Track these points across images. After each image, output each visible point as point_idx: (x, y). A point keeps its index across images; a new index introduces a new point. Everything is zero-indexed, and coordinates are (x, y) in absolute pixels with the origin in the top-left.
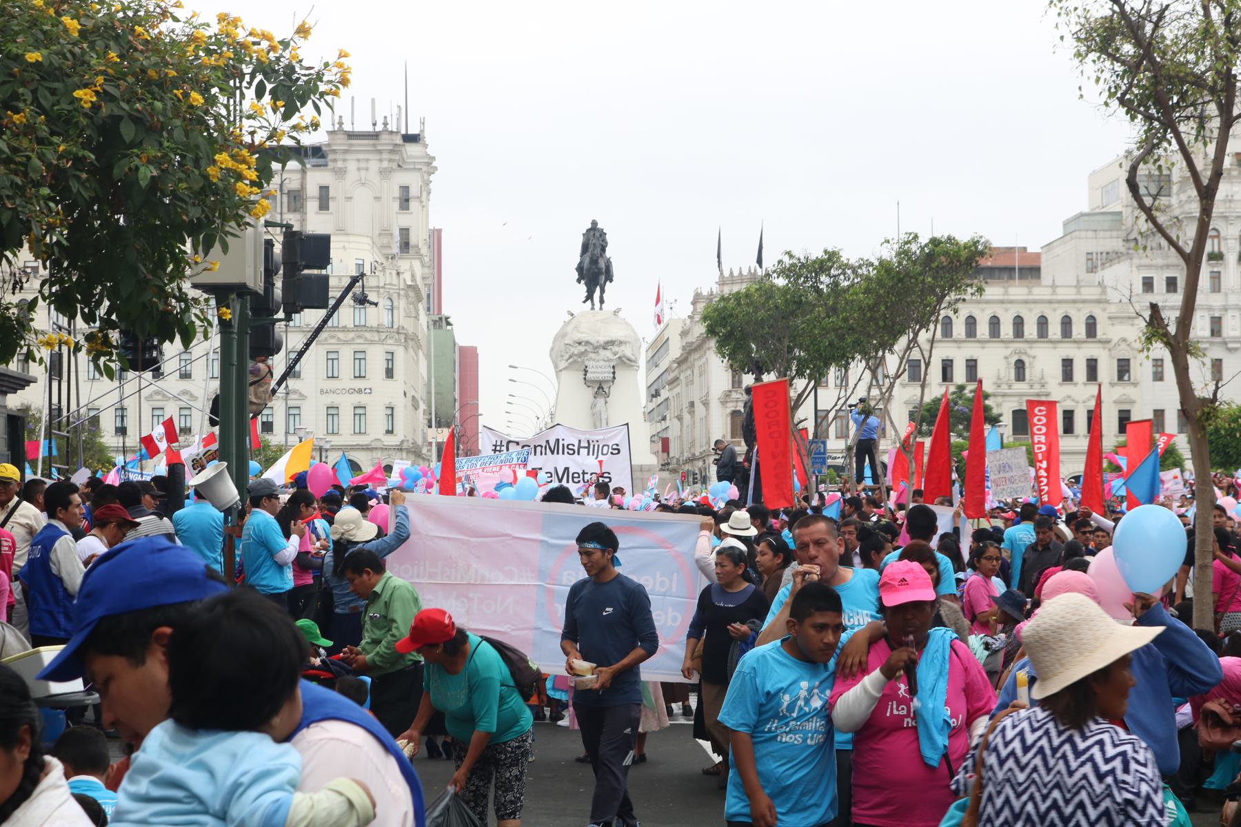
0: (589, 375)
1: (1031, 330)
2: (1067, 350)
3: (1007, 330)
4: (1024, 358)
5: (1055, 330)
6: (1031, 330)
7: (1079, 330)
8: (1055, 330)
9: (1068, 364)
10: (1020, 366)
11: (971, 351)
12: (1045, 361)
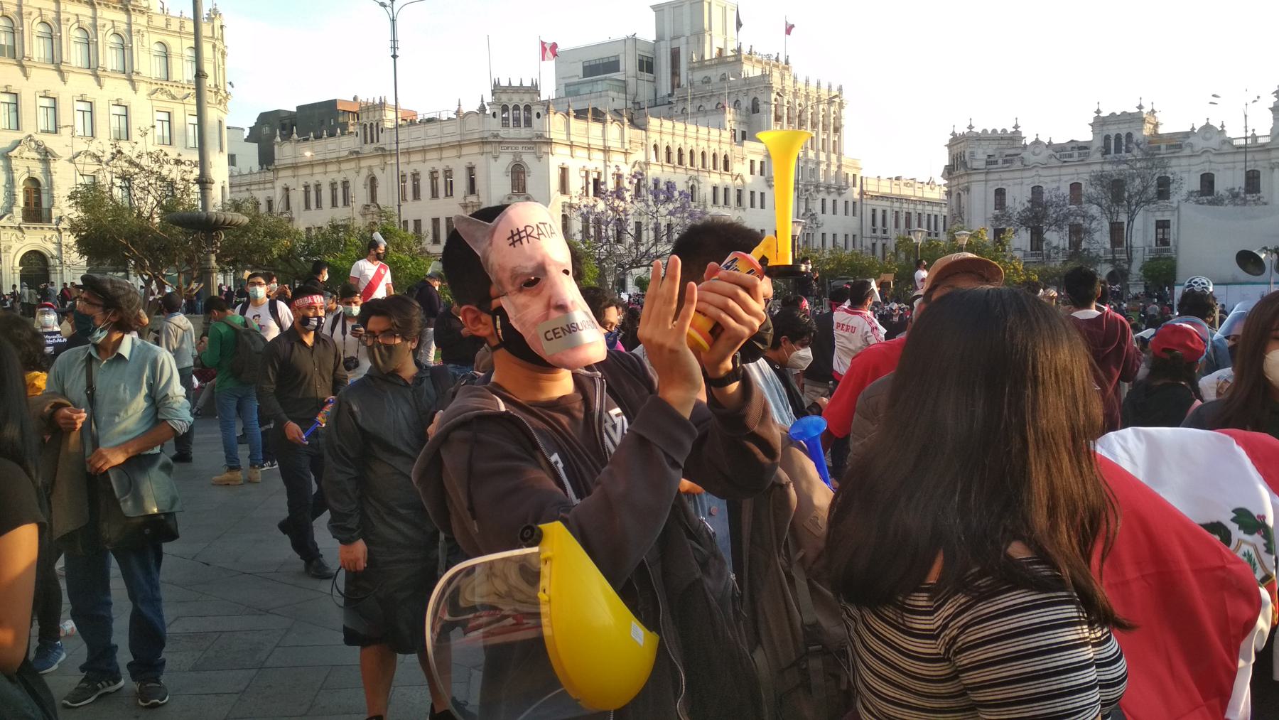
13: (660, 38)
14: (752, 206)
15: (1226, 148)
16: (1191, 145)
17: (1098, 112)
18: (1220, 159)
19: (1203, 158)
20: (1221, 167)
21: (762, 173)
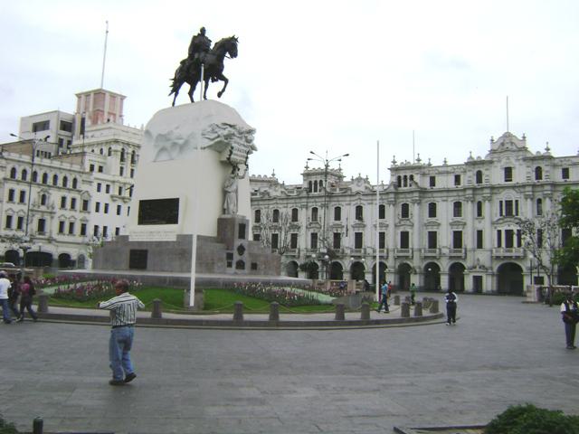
0: (232, 156)
1: (50, 181)
2: (64, 193)
3: (40, 179)
4: (47, 195)
5: (60, 182)
6: (50, 181)
7: (70, 184)
8: (60, 182)
9: (64, 199)
10: (44, 198)
11: (25, 187)
12: (55, 197)
13: (78, 112)
14: (97, 210)
15: (367, 192)
16: (350, 189)
17: (307, 167)
18: (365, 198)
19: (357, 197)
20: (365, 202)
21: (107, 192)
